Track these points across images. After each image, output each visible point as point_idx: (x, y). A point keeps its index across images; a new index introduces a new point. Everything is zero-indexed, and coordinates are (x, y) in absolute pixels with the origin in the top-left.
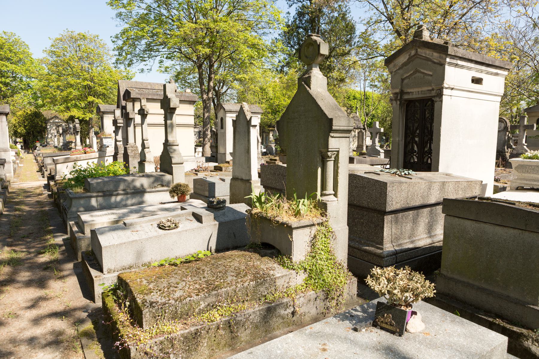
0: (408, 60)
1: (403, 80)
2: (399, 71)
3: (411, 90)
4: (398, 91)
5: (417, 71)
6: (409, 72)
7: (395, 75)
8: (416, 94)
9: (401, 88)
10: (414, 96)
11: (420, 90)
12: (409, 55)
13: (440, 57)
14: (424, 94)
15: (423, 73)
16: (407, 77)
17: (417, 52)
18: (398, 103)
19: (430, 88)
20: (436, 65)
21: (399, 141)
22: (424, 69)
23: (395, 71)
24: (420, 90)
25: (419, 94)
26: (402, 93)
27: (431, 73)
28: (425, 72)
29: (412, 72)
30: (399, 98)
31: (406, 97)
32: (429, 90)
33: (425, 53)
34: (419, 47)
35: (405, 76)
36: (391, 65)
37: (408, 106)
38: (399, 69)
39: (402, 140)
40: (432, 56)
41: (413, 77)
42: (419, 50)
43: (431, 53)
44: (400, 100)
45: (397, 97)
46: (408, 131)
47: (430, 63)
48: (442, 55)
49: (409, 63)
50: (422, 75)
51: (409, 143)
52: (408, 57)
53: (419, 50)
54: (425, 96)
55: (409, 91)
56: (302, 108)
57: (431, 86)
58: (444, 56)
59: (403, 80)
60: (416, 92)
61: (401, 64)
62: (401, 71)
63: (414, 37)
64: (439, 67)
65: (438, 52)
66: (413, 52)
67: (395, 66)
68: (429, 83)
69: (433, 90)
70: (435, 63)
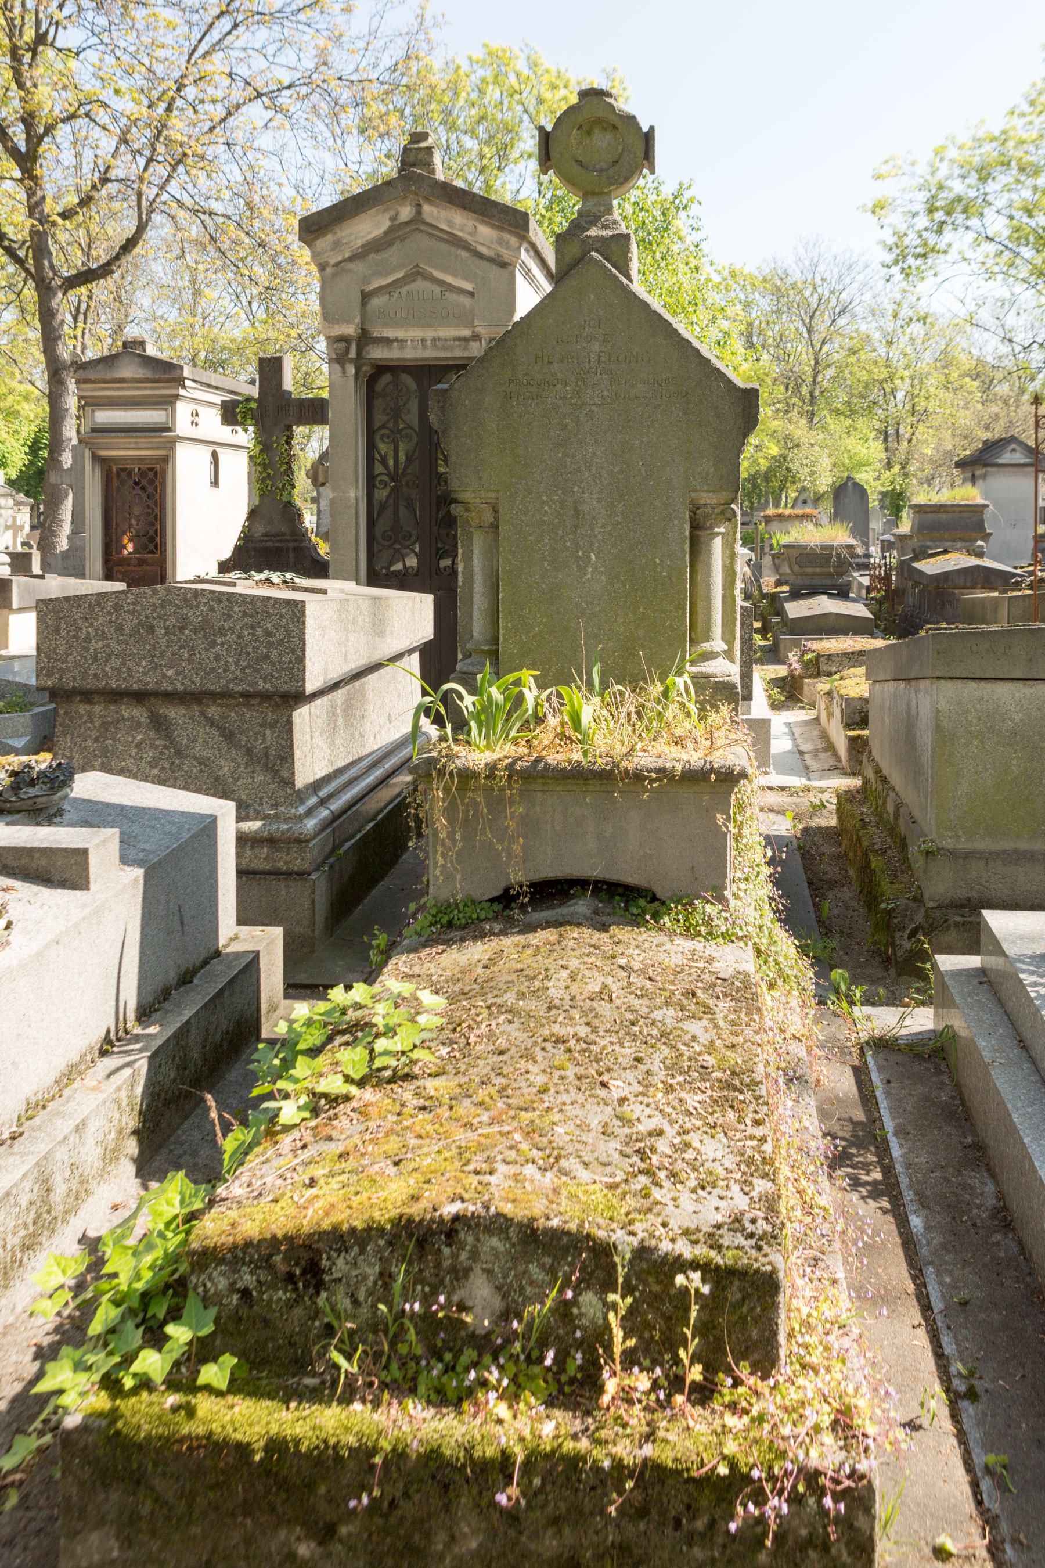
0: (387, 233)
1: (366, 297)
2: (351, 266)
3: (400, 334)
5: (417, 274)
6: (389, 274)
7: (335, 275)
9: (363, 321)
10: (410, 354)
11: (429, 333)
12: (393, 219)
13: (500, 242)
14: (444, 348)
15: (441, 283)
16: (381, 288)
17: (419, 213)
18: (351, 370)
19: (466, 332)
22: (446, 271)
23: (337, 265)
24: (429, 333)
25: (424, 347)
26: (364, 338)
27: (469, 287)
28: (449, 279)
29: (400, 275)
30: (353, 354)
31: (377, 353)
32: (459, 339)
33: (450, 223)
34: (426, 199)
35: (375, 285)
36: (324, 242)
38: (351, 259)
40: (474, 233)
41: (404, 290)
42: (427, 208)
43: (470, 223)
45: (347, 351)
46: (379, 468)
47: (464, 254)
48: (506, 236)
49: (390, 244)
50: (437, 289)
52: (386, 224)
53: (427, 208)
54: (448, 355)
55: (390, 333)
57: (471, 324)
58: (514, 241)
60: (412, 341)
61: (359, 243)
62: (359, 267)
64: (494, 271)
65: (493, 226)
66: (406, 213)
67: (336, 245)
68: (465, 318)
70: (480, 256)
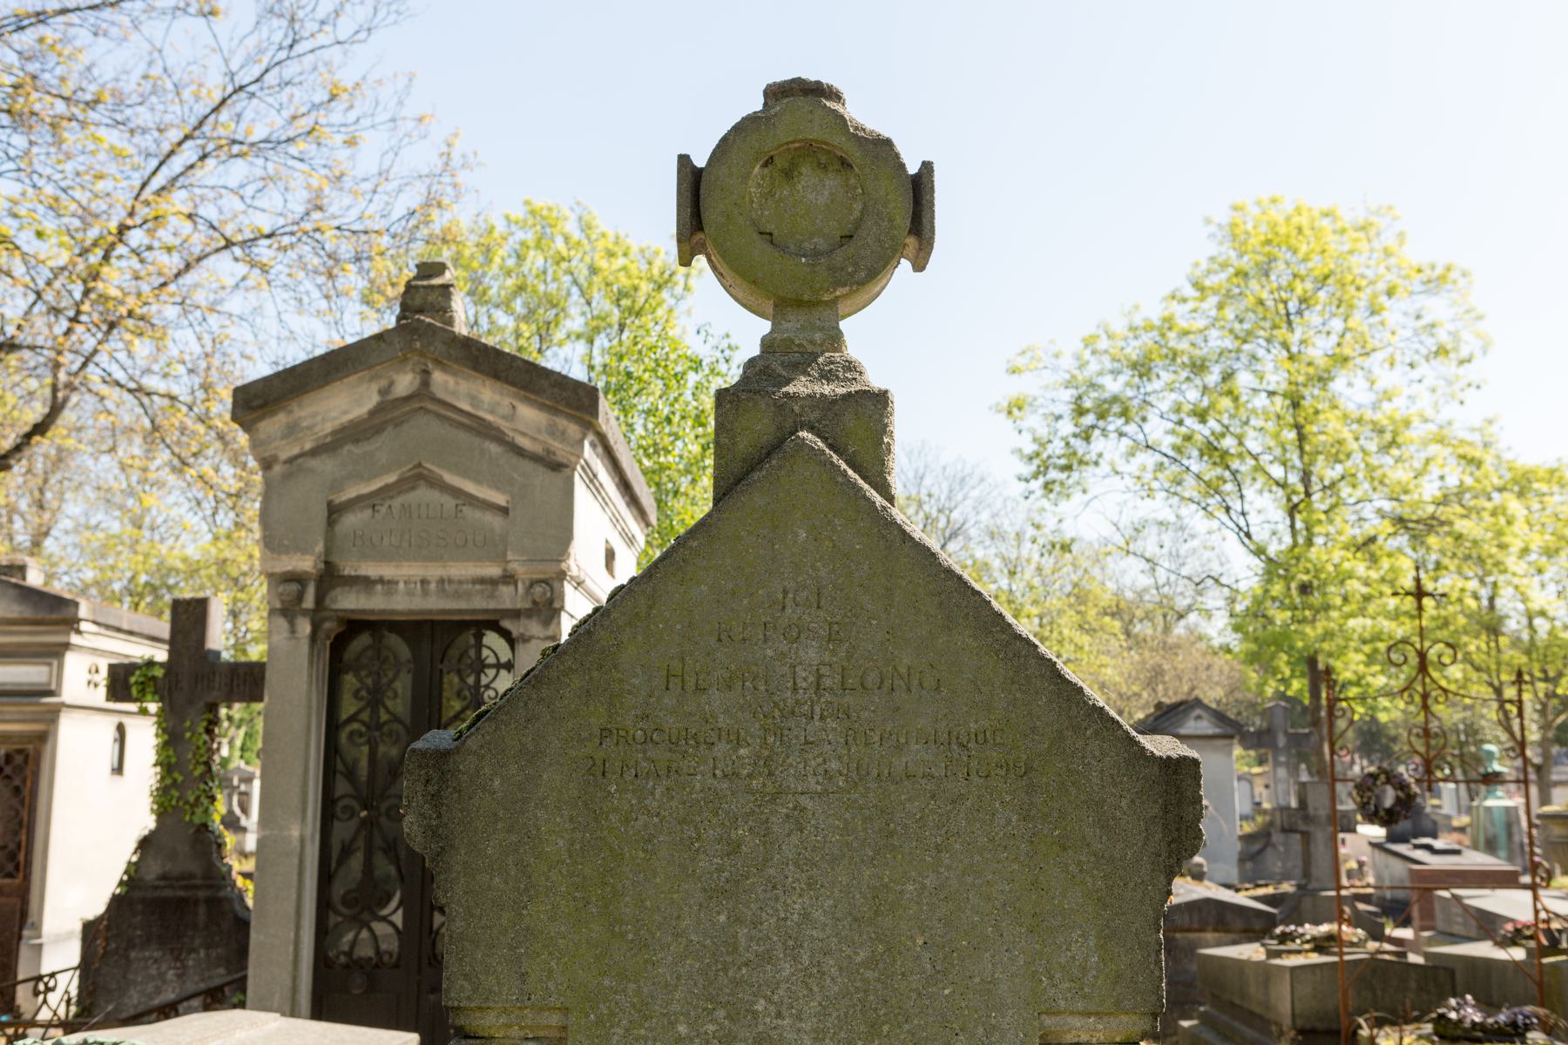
0: (373, 413)
1: (334, 512)
2: (314, 463)
3: (387, 571)
4: (306, 563)
5: (418, 477)
6: (374, 476)
7: (287, 477)
8: (410, 593)
9: (328, 550)
10: (402, 603)
11: (434, 571)
12: (383, 392)
13: (552, 431)
14: (457, 595)
15: (456, 492)
16: (359, 499)
17: (426, 383)
18: (305, 627)
19: (494, 571)
20: (527, 466)
21: (302, 840)
22: (465, 474)
23: (291, 461)
24: (434, 571)
25: (425, 593)
26: (329, 577)
27: (500, 499)
28: (470, 487)
29: (391, 478)
30: (309, 602)
31: (349, 601)
32: (482, 581)
33: (474, 400)
34: (438, 363)
35: (351, 493)
36: (272, 426)
37: (339, 645)
38: (314, 453)
39: (313, 836)
40: (511, 416)
41: (397, 502)
42: (438, 377)
43: (506, 401)
44: (318, 615)
45: (300, 597)
46: (342, 787)
47: (494, 448)
48: (562, 422)
49: (379, 430)
50: (449, 502)
51: (346, 851)
52: (373, 400)
53: (438, 377)
54: (463, 605)
55: (371, 570)
56: (811, 653)
57: (502, 558)
58: (573, 429)
59: (334, 512)
60: (405, 583)
61: (329, 427)
62: (327, 466)
63: (405, 307)
64: (541, 476)
65: (542, 407)
66: (405, 383)
67: (292, 430)
68: (494, 548)
69: (509, 578)
70: (519, 452)
